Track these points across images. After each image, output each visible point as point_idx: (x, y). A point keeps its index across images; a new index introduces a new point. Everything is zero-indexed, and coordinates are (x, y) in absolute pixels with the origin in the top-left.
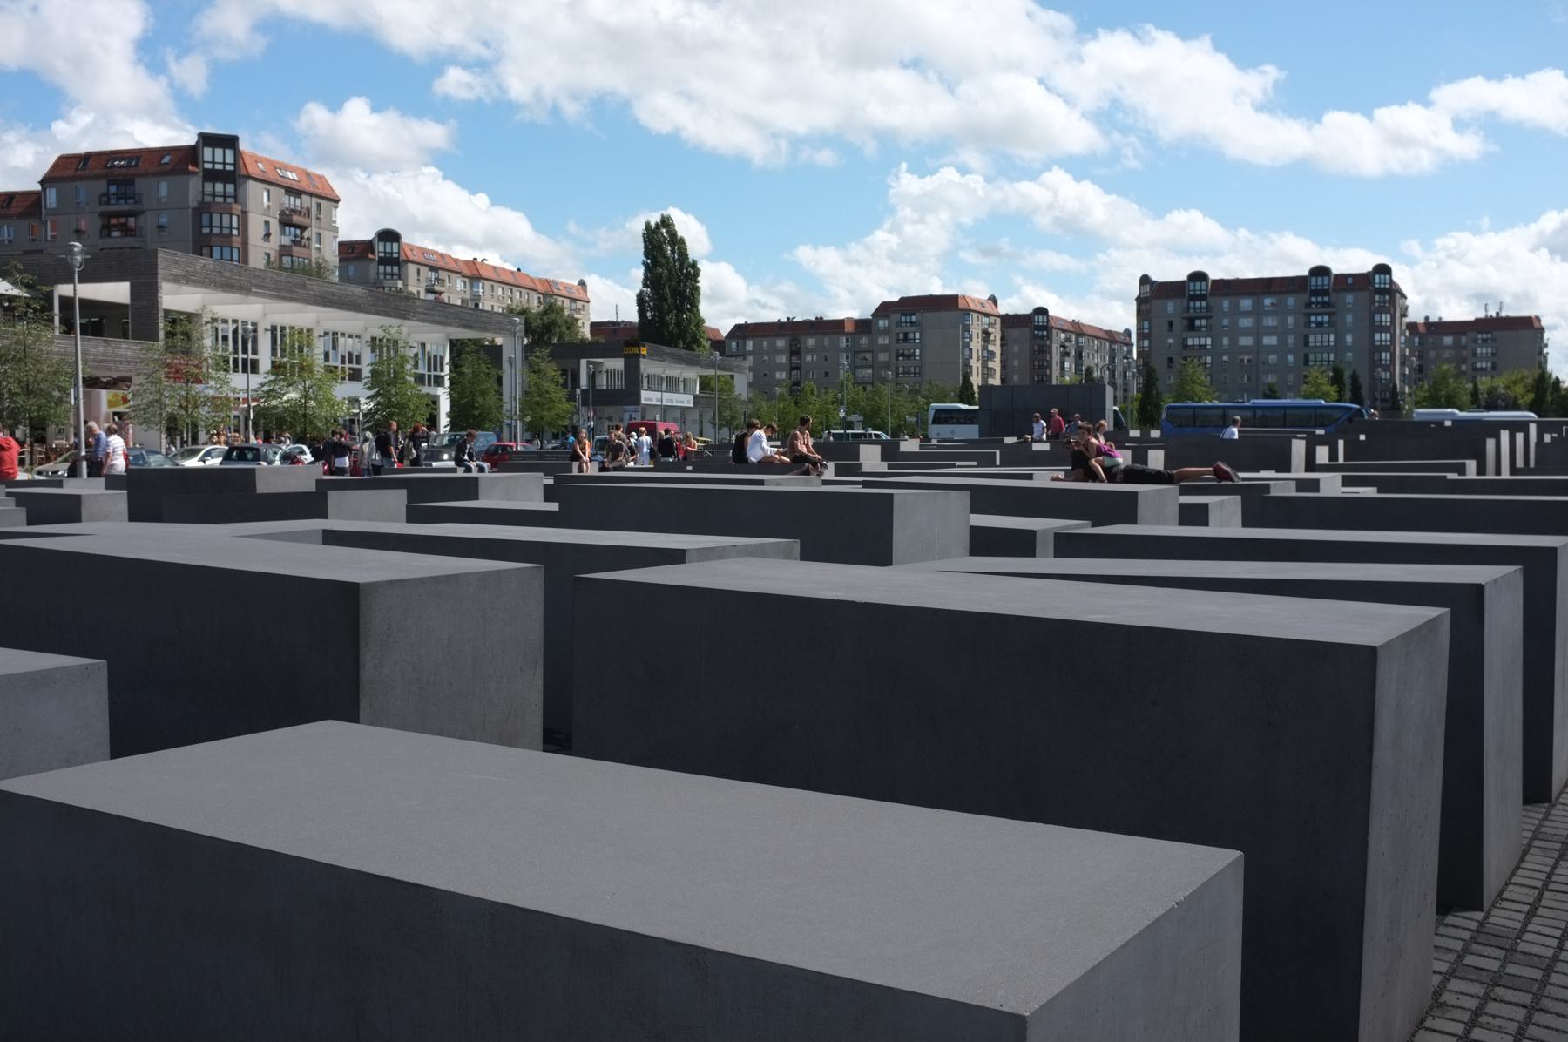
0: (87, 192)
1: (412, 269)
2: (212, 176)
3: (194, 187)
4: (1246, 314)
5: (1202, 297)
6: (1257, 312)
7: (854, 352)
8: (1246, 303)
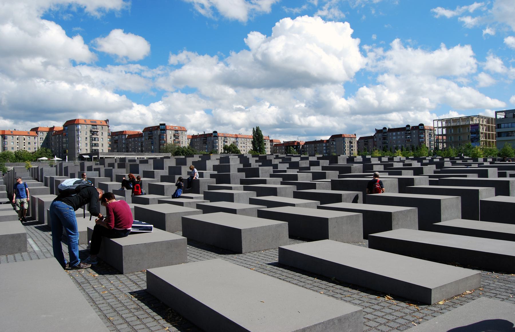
0: (147, 133)
1: (220, 138)
2: (161, 130)
3: (159, 132)
4: (394, 136)
5: (386, 133)
6: (396, 135)
7: (326, 147)
8: (394, 134)
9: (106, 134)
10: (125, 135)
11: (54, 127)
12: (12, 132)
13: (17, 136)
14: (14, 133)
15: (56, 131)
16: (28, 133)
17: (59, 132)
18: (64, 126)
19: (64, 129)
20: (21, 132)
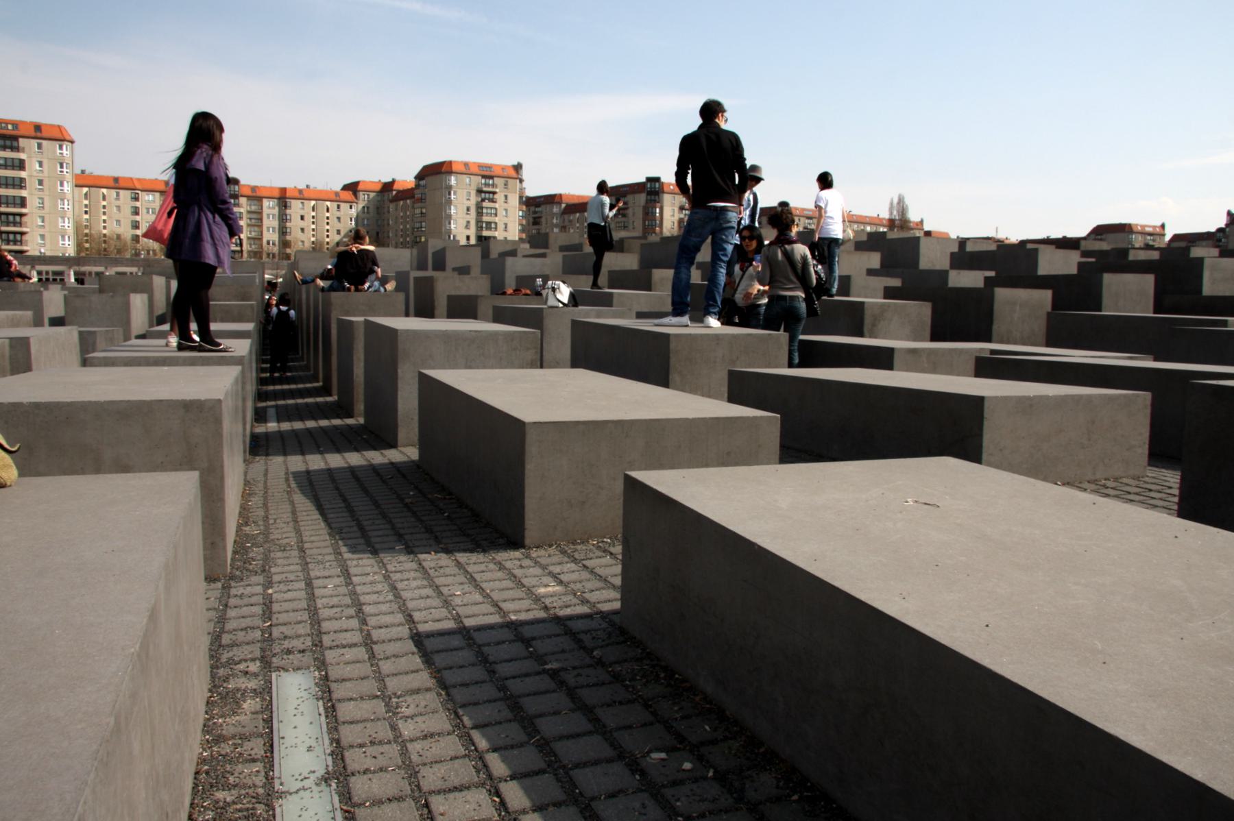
9: (514, 201)
10: (560, 203)
11: (393, 182)
12: (300, 191)
13: (313, 203)
14: (306, 196)
15: (399, 192)
16: (337, 194)
17: (406, 194)
18: (420, 177)
19: (418, 186)
20: (321, 191)
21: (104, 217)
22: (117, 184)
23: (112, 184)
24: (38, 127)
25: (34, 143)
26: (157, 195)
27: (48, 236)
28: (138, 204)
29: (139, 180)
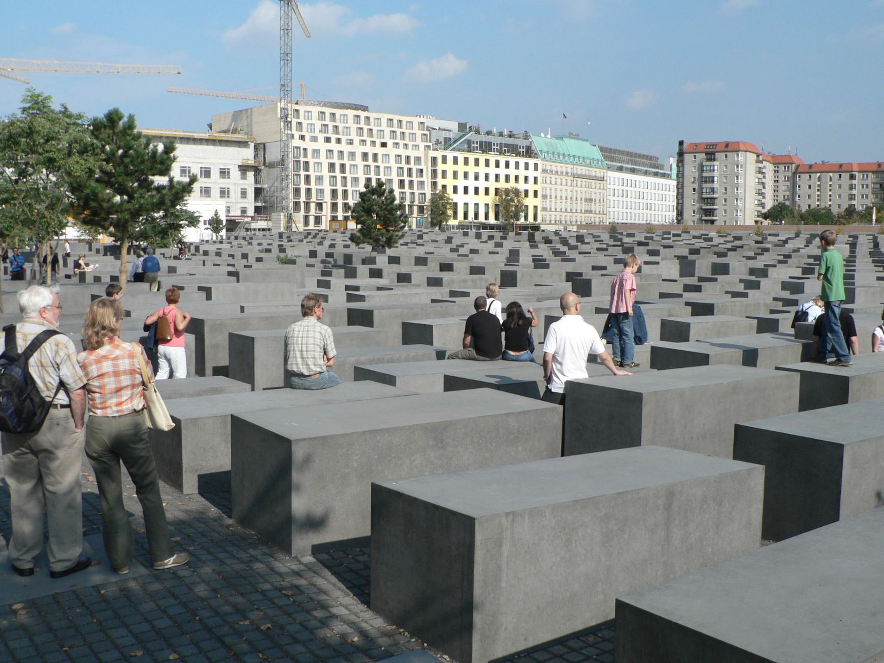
21: (830, 193)
22: (840, 169)
23: (837, 169)
24: (727, 145)
25: (723, 155)
26: (870, 174)
27: (728, 211)
28: (854, 182)
29: (859, 164)
